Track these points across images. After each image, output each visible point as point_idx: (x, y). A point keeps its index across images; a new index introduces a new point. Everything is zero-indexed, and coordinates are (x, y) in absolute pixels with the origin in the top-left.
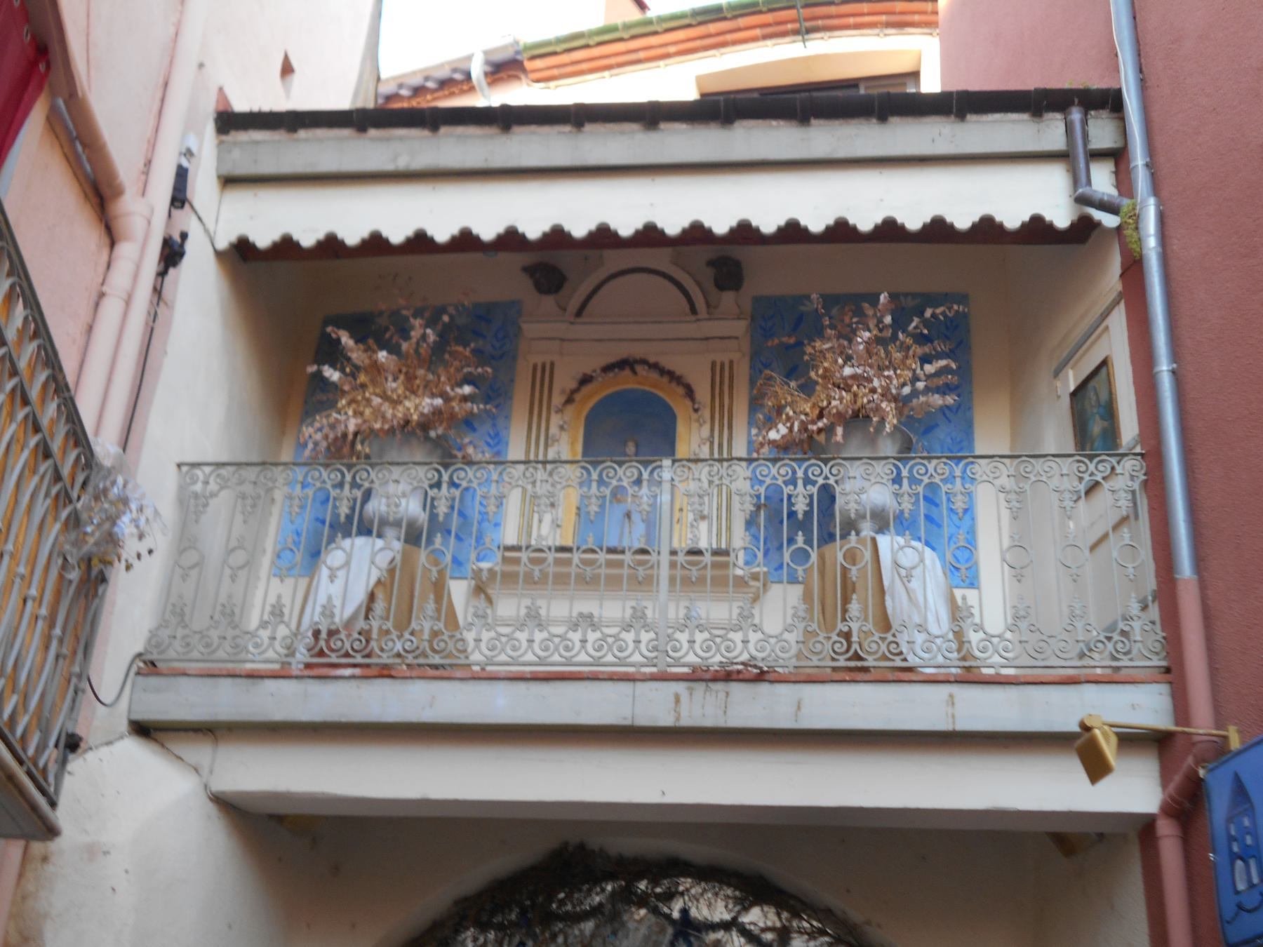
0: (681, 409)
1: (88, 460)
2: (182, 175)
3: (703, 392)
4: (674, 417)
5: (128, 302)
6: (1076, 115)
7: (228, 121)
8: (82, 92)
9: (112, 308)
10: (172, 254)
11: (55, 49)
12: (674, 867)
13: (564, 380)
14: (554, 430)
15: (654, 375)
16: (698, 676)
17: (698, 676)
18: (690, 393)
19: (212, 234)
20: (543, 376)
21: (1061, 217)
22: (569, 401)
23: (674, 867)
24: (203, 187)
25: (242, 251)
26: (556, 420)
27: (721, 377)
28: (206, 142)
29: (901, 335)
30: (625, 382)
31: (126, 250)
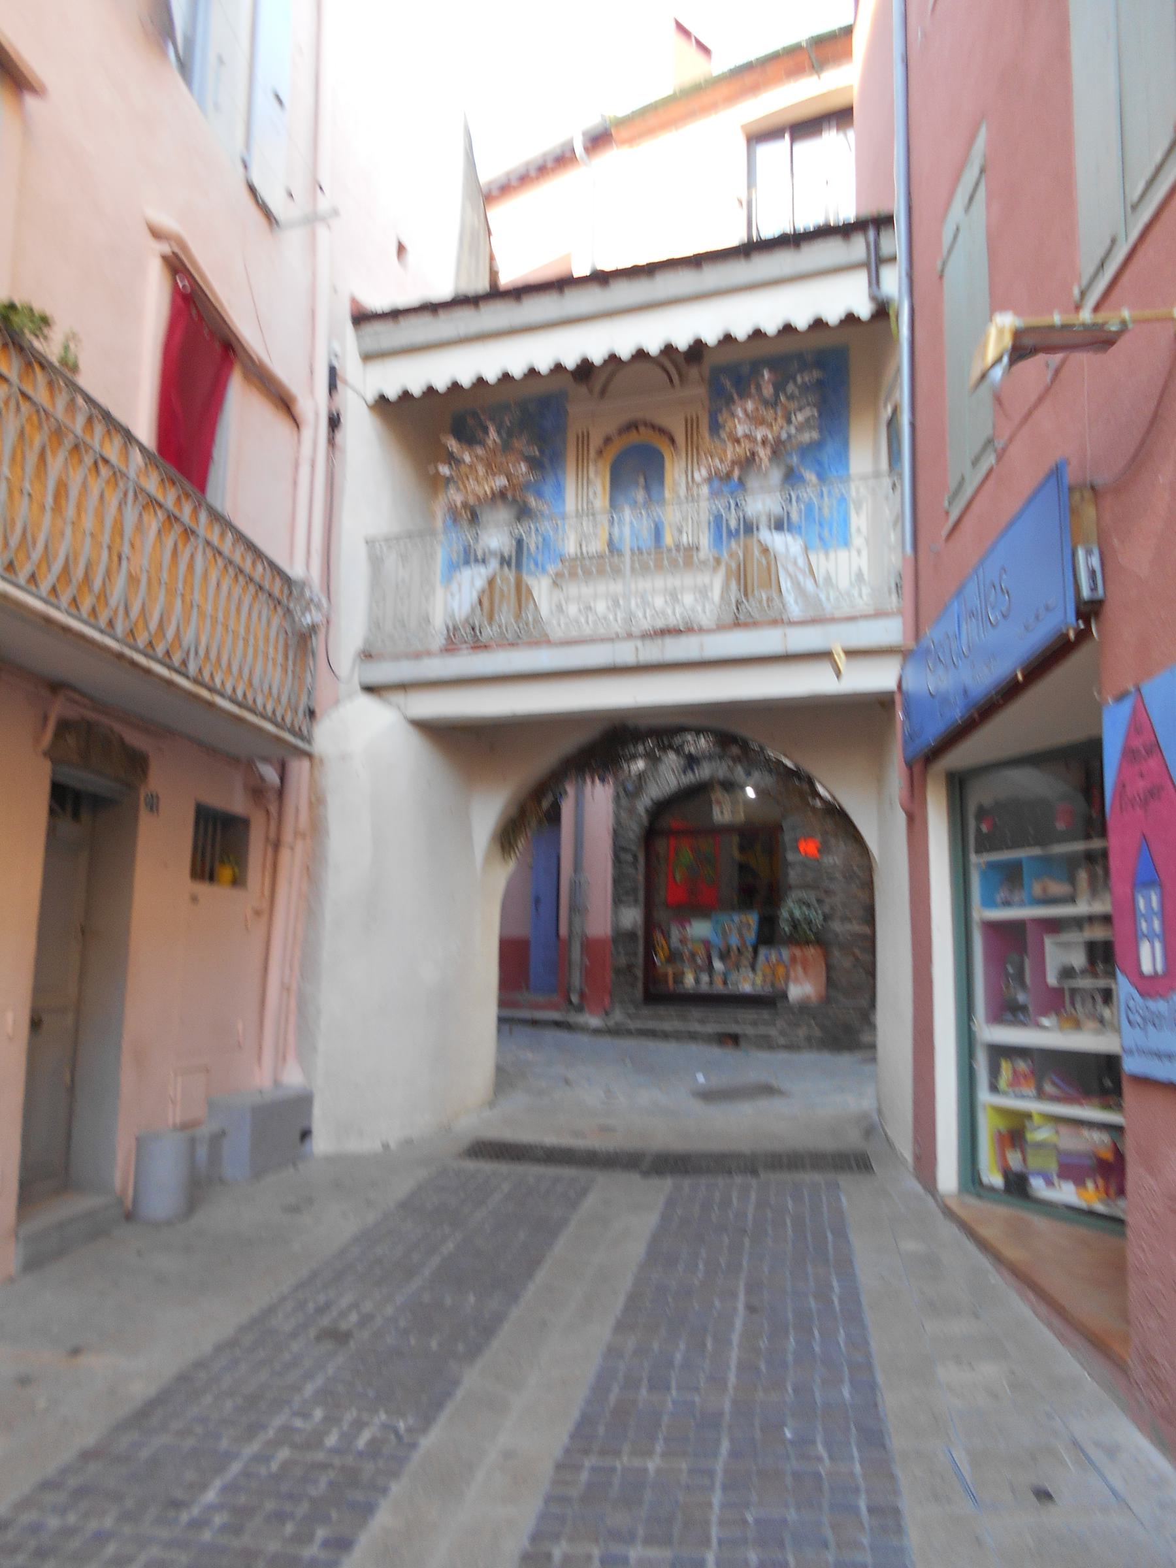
0: (667, 452)
1: (287, 580)
2: (333, 373)
3: (680, 439)
4: (663, 457)
5: (313, 466)
6: (871, 233)
7: (361, 318)
8: (257, 355)
9: (304, 470)
10: (334, 422)
11: (235, 343)
12: (681, 730)
13: (596, 441)
14: (592, 475)
15: (650, 432)
16: (646, 636)
17: (646, 636)
18: (672, 440)
19: (363, 394)
20: (583, 440)
21: (864, 310)
22: (600, 453)
23: (681, 730)
24: (351, 367)
25: (382, 404)
26: (592, 469)
27: (691, 427)
28: (349, 343)
29: (782, 398)
30: (633, 438)
31: (307, 433)
